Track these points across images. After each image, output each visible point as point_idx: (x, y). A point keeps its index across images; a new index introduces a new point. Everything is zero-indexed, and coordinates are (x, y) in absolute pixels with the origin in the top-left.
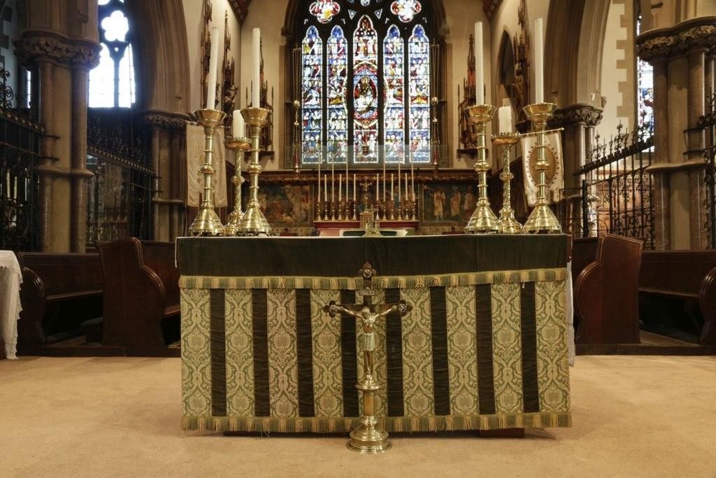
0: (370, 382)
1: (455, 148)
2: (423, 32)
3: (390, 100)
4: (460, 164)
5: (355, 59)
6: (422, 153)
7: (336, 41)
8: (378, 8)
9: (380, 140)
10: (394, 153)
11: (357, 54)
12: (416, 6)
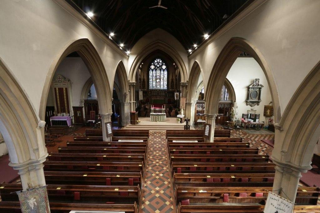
0: (158, 120)
1: (170, 87)
3: (161, 80)
4: (170, 90)
6: (166, 87)
7: (154, 72)
9: (160, 86)
10: (162, 88)
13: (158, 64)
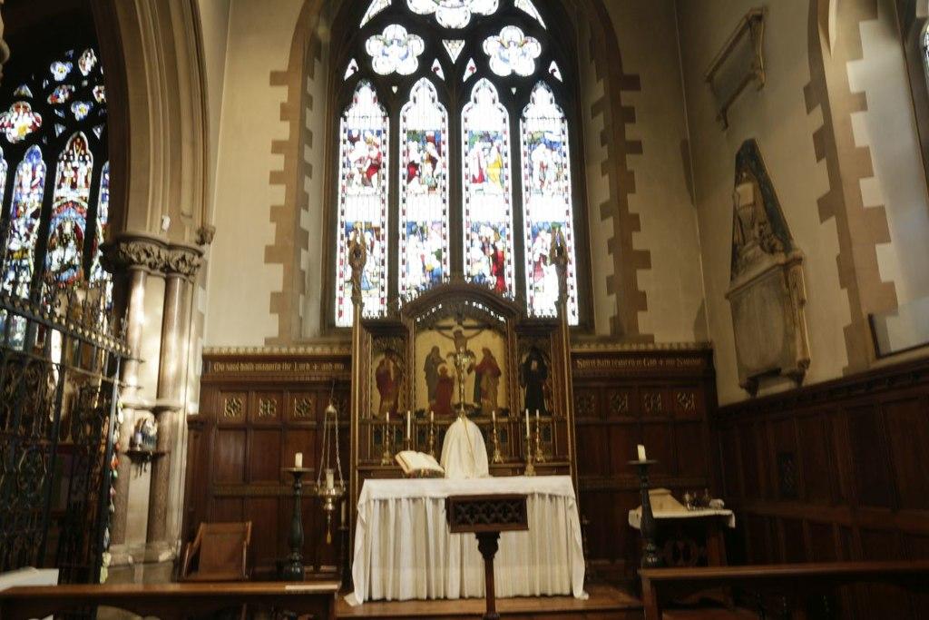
5: (57, 193)
7: (31, 170)
8: (97, 124)
11: (60, 187)
13: (83, 95)
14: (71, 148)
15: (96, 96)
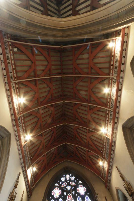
2: (89, 198)
12: (84, 189)
13: (68, 184)
14: (68, 198)
15: (71, 184)
